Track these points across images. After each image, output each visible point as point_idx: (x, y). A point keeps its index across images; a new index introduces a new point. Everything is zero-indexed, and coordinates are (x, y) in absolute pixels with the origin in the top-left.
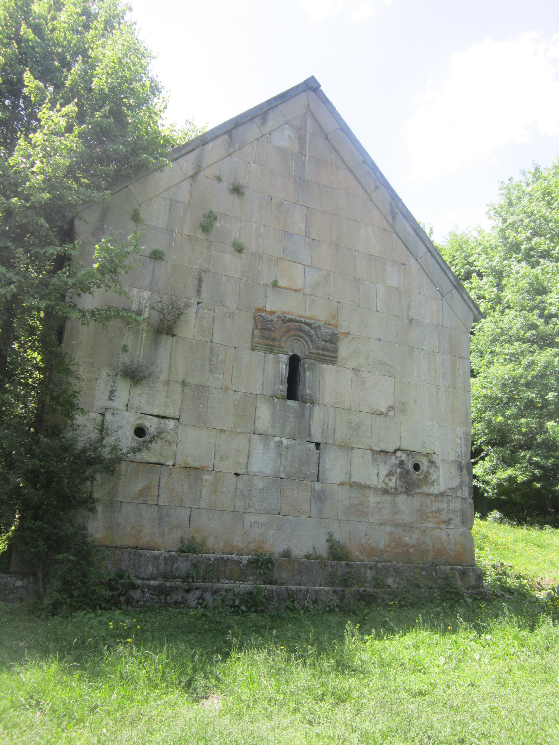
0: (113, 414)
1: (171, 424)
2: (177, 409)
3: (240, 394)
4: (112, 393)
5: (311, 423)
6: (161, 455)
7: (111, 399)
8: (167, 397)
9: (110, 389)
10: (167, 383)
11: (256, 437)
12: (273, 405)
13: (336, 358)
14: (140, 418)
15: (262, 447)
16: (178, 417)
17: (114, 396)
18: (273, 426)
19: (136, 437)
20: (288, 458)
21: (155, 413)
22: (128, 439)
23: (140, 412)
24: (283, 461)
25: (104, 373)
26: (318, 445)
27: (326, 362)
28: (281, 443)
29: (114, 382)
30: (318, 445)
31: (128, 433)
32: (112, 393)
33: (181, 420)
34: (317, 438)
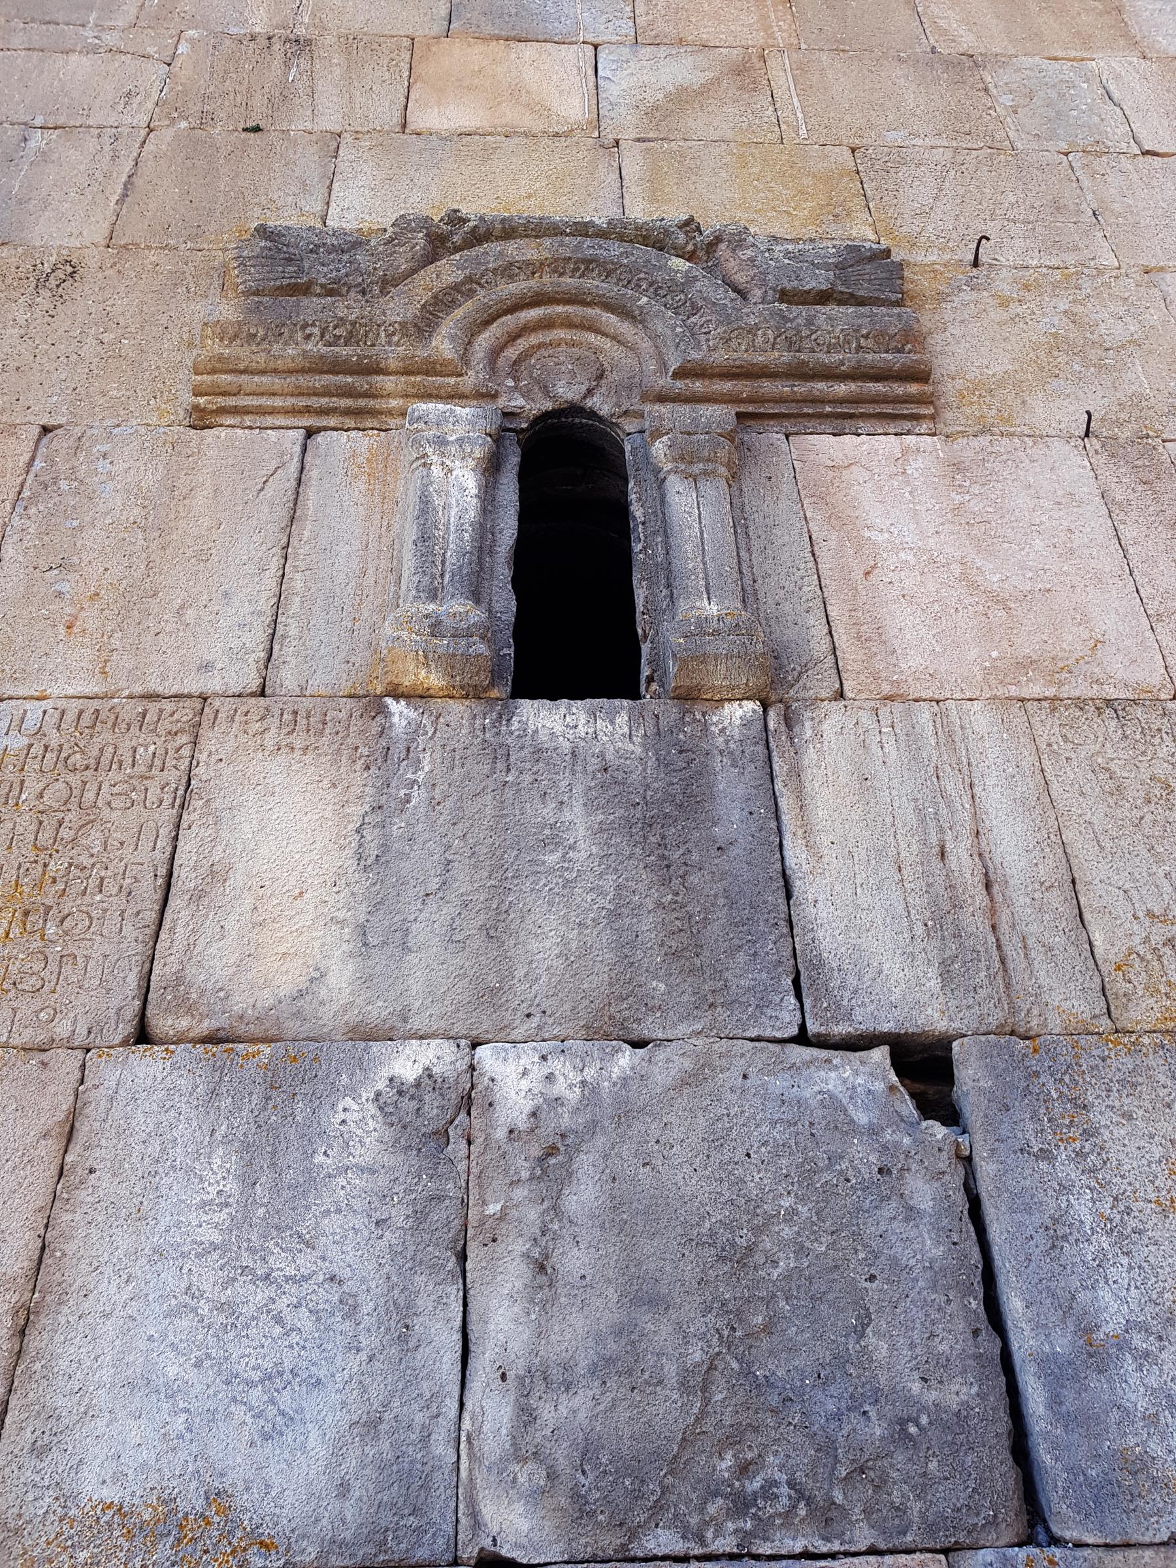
3: (34, 710)
5: (796, 855)
11: (147, 1065)
12: (386, 757)
13: (922, 376)
15: (220, 1173)
18: (378, 936)
20: (573, 1261)
24: (504, 1323)
26: (924, 1068)
27: (843, 418)
28: (469, 1098)
30: (924, 1068)
34: (901, 988)
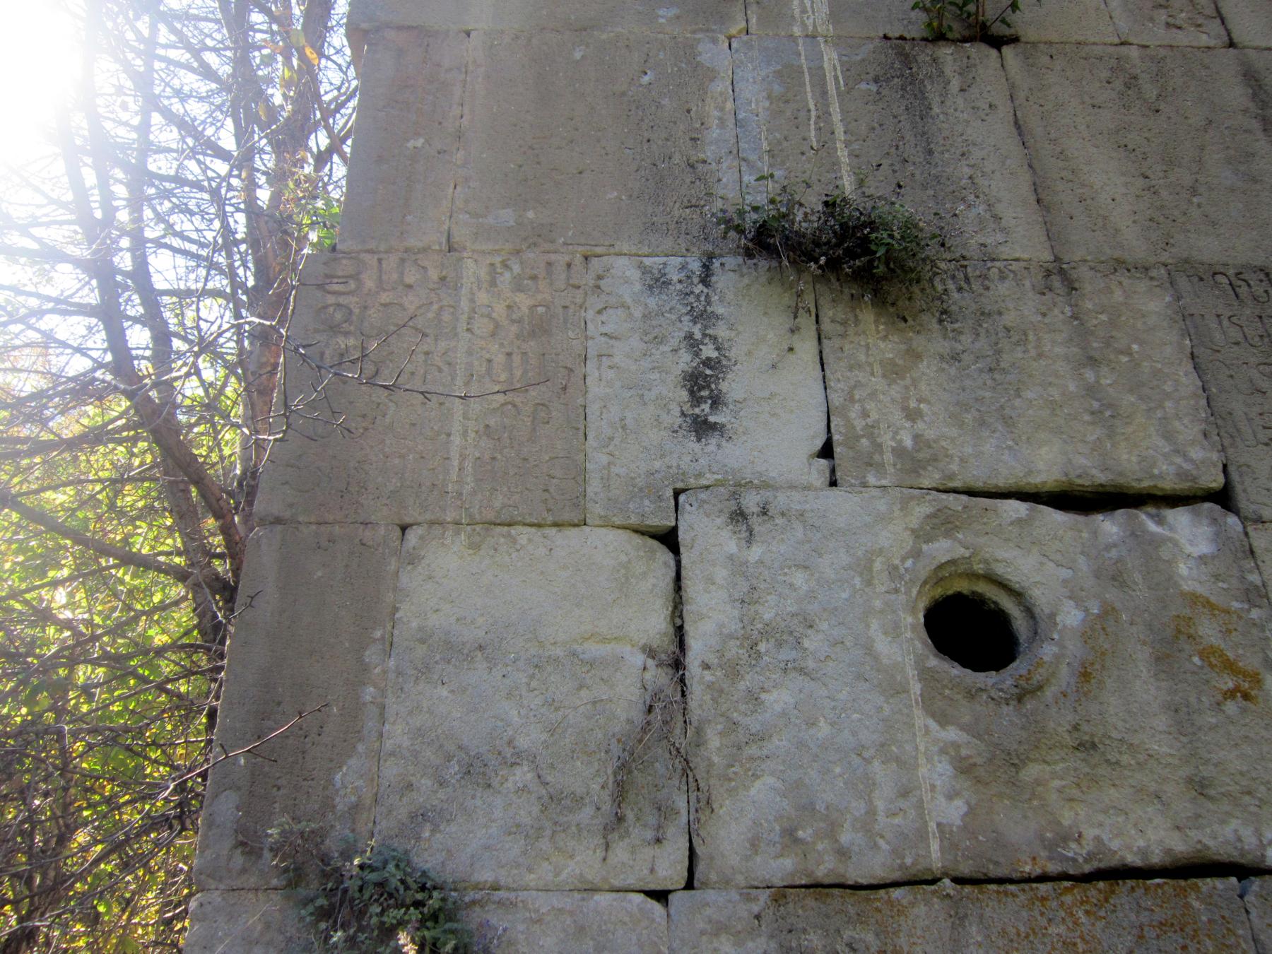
0: (739, 516)
1: (1189, 533)
2: (1188, 430)
4: (702, 383)
6: (1200, 787)
7: (702, 428)
8: (1093, 361)
9: (685, 361)
10: (1059, 276)
14: (942, 524)
16: (1215, 481)
17: (716, 402)
19: (956, 670)
21: (1047, 467)
22: (898, 690)
23: (931, 478)
25: (625, 273)
29: (703, 316)
31: (883, 646)
32: (702, 383)
33: (1249, 495)
